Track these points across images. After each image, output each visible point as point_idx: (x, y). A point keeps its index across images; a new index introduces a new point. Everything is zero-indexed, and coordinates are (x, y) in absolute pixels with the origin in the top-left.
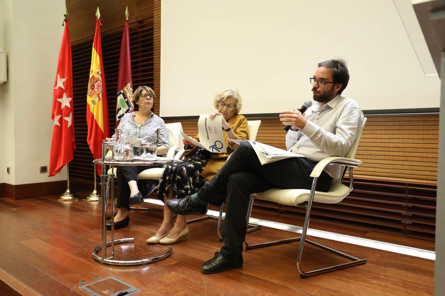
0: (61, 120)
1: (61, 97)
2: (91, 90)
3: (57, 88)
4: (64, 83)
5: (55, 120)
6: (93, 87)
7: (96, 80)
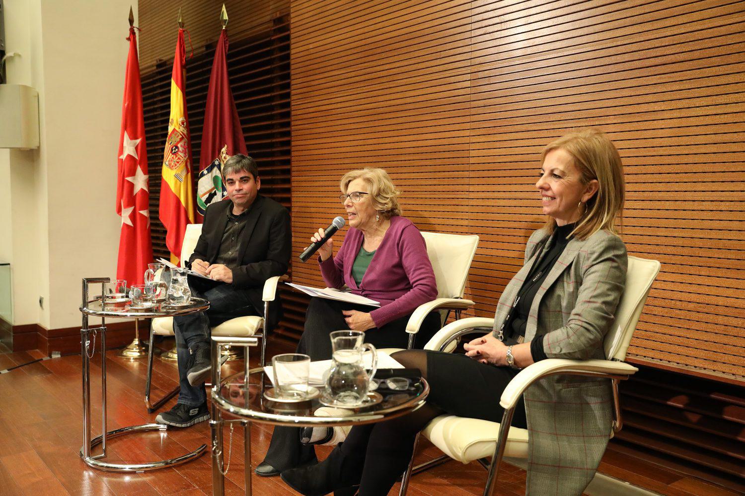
0: (133, 217)
1: (133, 173)
2: (171, 156)
3: (124, 157)
4: (136, 148)
5: (122, 215)
6: (175, 149)
7: (180, 137)
